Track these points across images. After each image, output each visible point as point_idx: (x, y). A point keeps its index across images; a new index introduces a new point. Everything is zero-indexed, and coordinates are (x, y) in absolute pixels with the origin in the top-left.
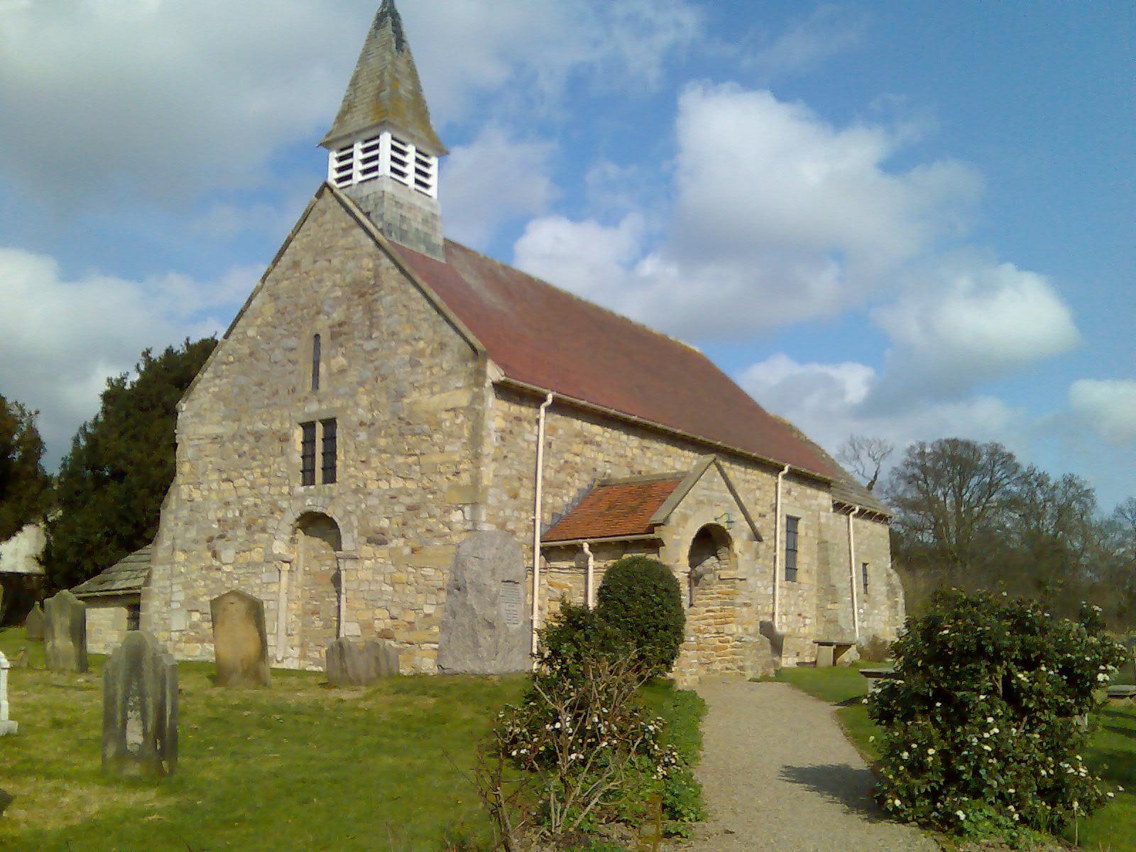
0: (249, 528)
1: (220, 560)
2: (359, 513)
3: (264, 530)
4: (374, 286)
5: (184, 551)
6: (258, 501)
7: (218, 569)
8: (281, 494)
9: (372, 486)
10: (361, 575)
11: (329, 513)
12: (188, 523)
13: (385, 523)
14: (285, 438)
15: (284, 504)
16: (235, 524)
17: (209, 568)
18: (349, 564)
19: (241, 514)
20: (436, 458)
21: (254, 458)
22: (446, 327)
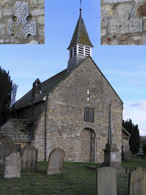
0: (70, 129)
1: (62, 136)
2: (99, 129)
3: (75, 130)
4: (102, 83)
5: (50, 133)
6: (73, 123)
7: (62, 138)
8: (79, 122)
9: (102, 124)
10: (100, 142)
11: (93, 128)
12: (52, 126)
13: (105, 132)
14: (81, 110)
15: (80, 125)
16: (66, 128)
17: (59, 138)
18: (98, 140)
19: (68, 126)
20: (116, 121)
21: (72, 113)
22: (117, 97)
